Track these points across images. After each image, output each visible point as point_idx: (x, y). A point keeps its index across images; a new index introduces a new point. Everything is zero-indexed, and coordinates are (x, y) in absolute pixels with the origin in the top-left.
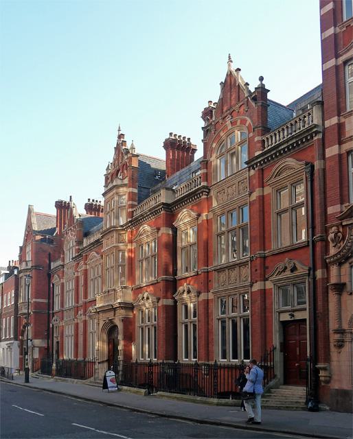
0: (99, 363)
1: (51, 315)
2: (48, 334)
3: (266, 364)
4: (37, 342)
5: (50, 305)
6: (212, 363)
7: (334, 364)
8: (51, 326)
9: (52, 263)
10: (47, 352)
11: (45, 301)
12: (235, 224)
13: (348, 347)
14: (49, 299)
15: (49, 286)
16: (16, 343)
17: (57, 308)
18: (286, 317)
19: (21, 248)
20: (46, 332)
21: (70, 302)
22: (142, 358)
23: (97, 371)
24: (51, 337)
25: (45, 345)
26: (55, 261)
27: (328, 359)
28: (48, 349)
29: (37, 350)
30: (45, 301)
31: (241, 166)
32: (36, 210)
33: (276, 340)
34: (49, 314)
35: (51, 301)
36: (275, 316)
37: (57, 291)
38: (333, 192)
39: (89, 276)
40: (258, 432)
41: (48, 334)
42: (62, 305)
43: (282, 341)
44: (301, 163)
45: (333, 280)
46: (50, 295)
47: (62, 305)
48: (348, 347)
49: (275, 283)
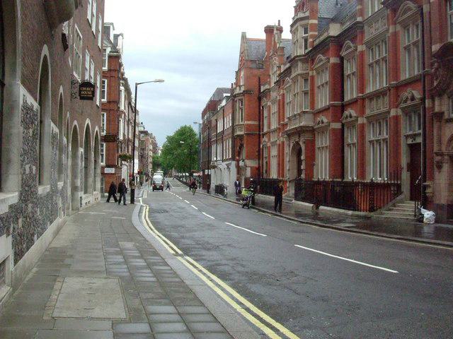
0: (290, 182)
1: (262, 136)
2: (259, 154)
3: (396, 182)
4: (248, 163)
5: (260, 127)
6: (368, 180)
7: (437, 181)
8: (261, 146)
9: (262, 87)
10: (258, 171)
11: (256, 123)
12: (324, 82)
13: (446, 167)
14: (259, 120)
15: (260, 109)
16: (234, 163)
17: (266, 130)
18: (410, 141)
19: (237, 72)
20: (259, 154)
21: (274, 126)
22: (380, 177)
23: (288, 189)
24: (261, 157)
25: (257, 166)
26: (264, 85)
27: (432, 178)
28: (258, 169)
29: (249, 169)
30: (256, 123)
31: (378, 6)
32: (248, 36)
33: (404, 160)
34: (259, 135)
35: (261, 123)
36: (402, 139)
37: (266, 114)
38: (436, 34)
39: (285, 100)
40: (428, 245)
41: (259, 154)
42: (269, 127)
43: (409, 161)
44: (380, 21)
45: (437, 110)
46: (260, 117)
47: (269, 127)
48: (446, 167)
49: (403, 109)
